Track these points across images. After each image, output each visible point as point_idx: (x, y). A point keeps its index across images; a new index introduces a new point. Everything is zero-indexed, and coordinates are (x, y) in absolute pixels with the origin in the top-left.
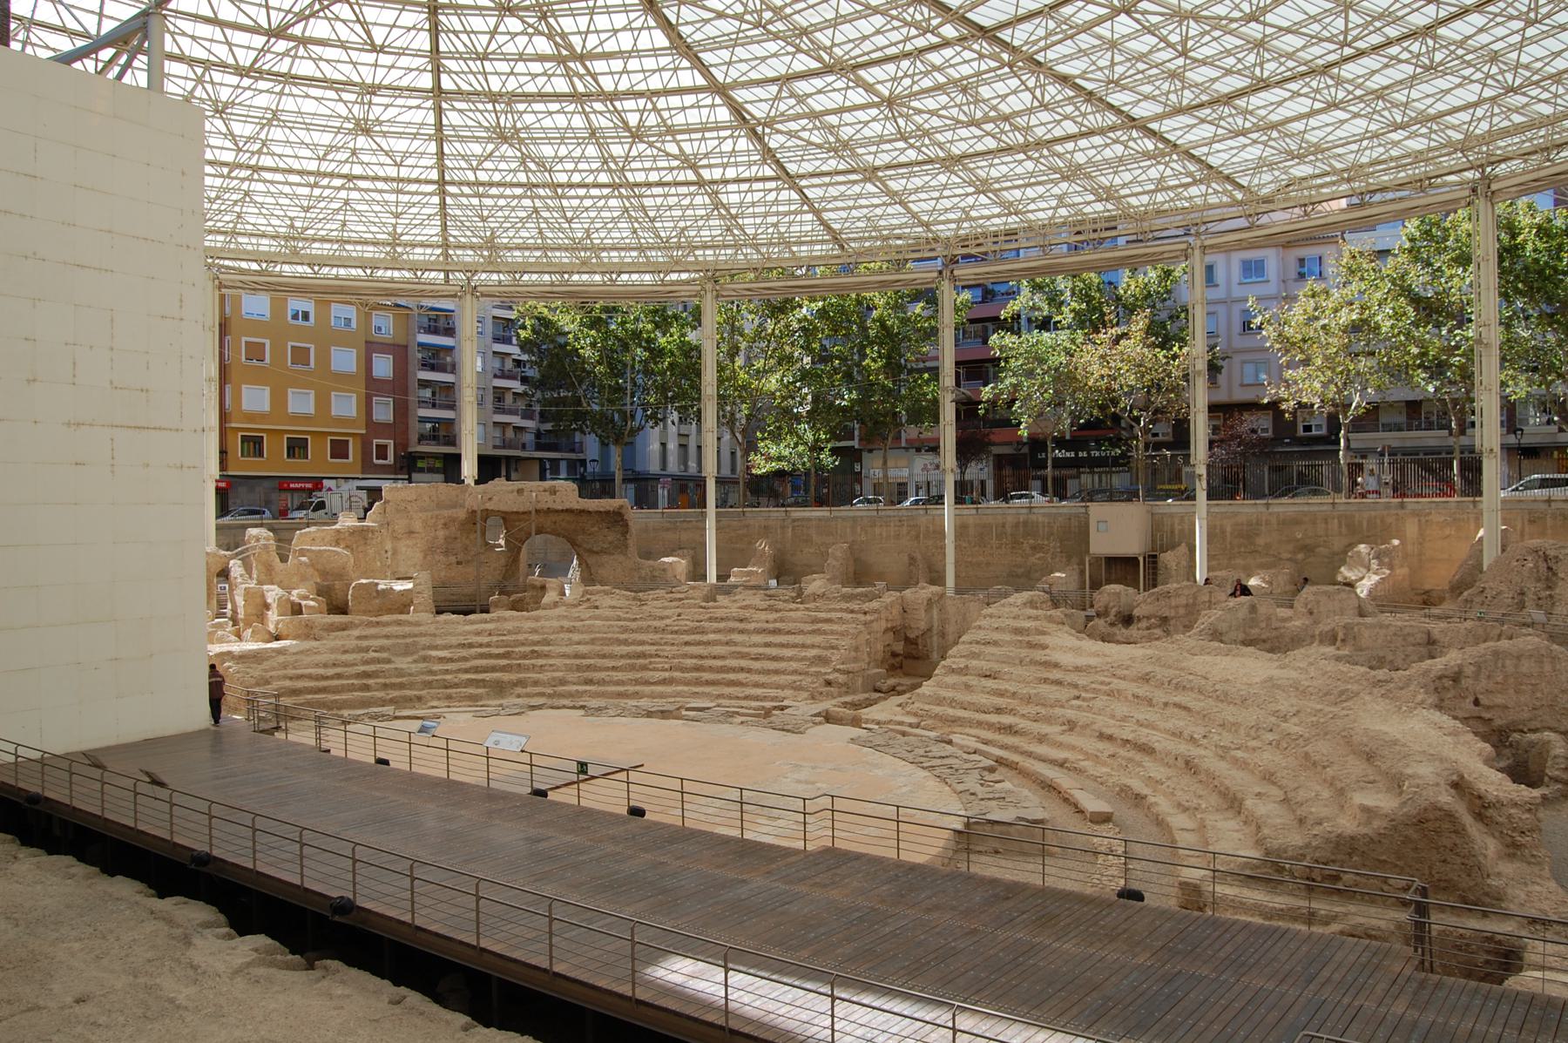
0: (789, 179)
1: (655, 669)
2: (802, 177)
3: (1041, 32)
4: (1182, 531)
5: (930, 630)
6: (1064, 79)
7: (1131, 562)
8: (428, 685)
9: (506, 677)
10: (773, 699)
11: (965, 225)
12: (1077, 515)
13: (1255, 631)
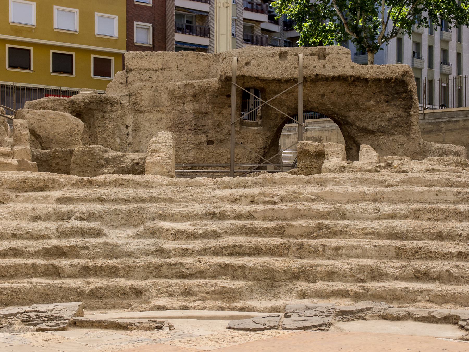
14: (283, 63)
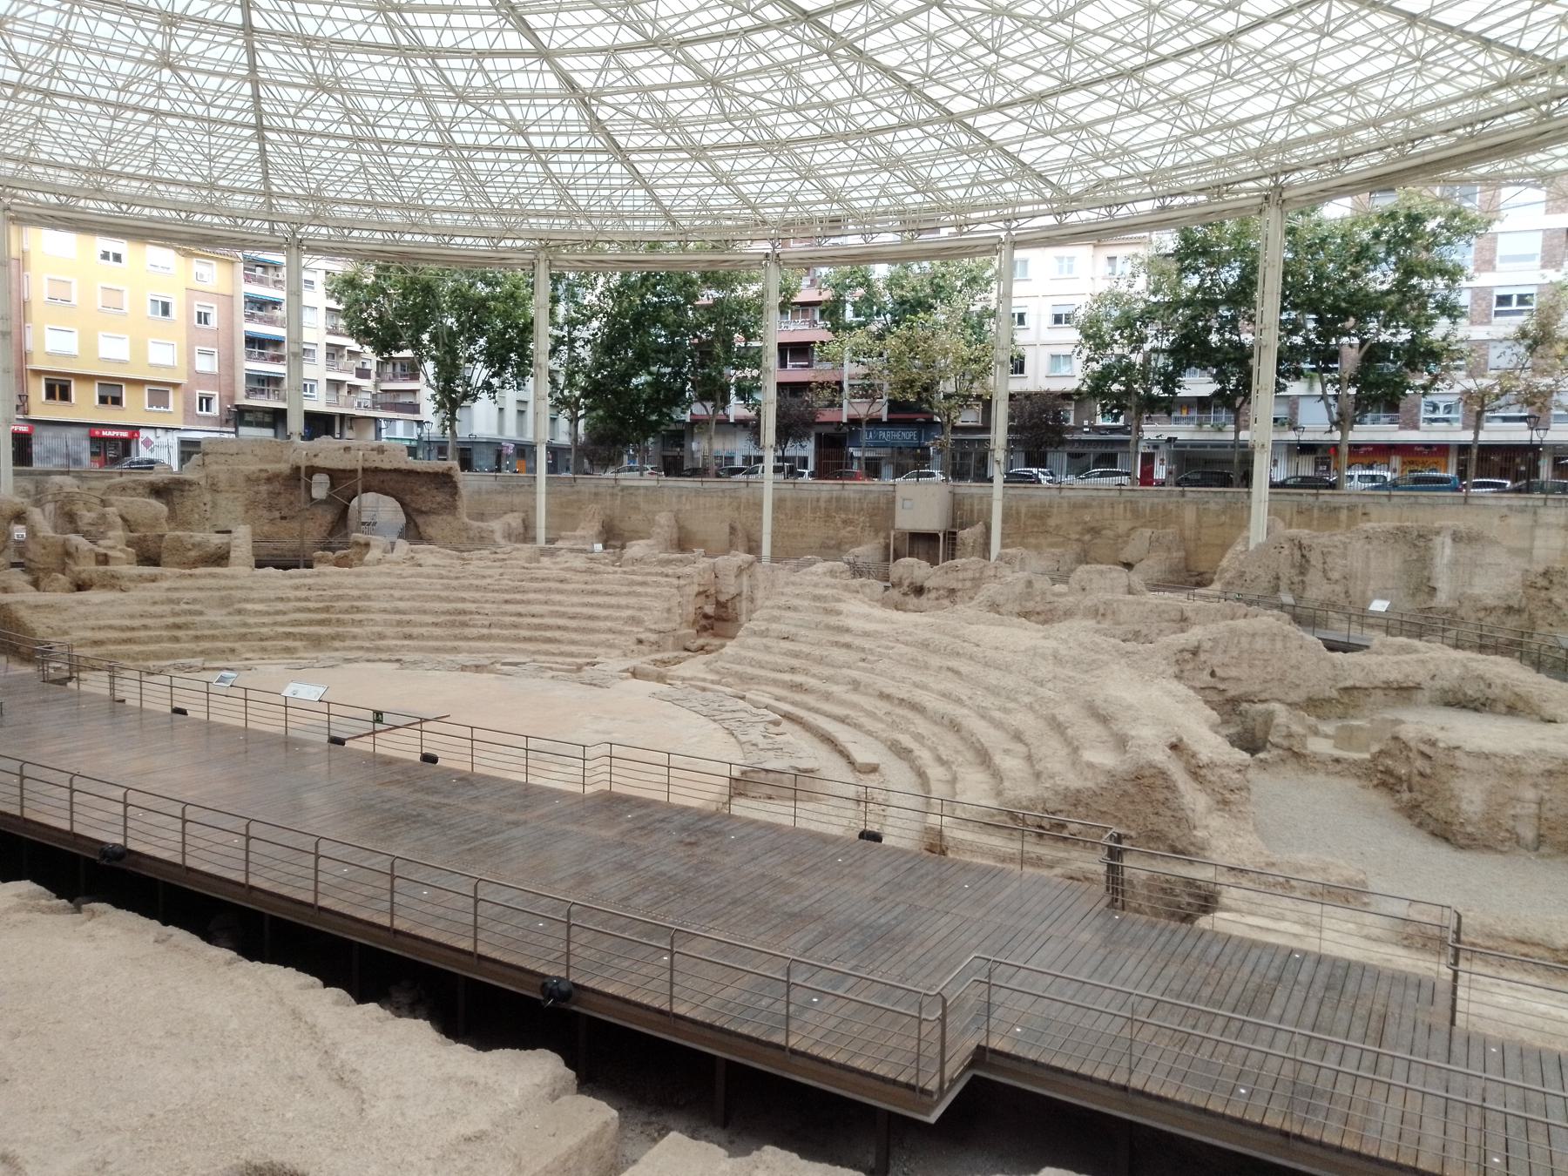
0: (620, 153)
1: (474, 626)
2: (633, 151)
3: (861, 20)
4: (980, 511)
5: (739, 595)
6: (885, 71)
7: (931, 538)
8: (243, 637)
9: (324, 630)
10: (587, 655)
11: (791, 209)
12: (885, 493)
13: (1030, 605)
14: (347, 456)
